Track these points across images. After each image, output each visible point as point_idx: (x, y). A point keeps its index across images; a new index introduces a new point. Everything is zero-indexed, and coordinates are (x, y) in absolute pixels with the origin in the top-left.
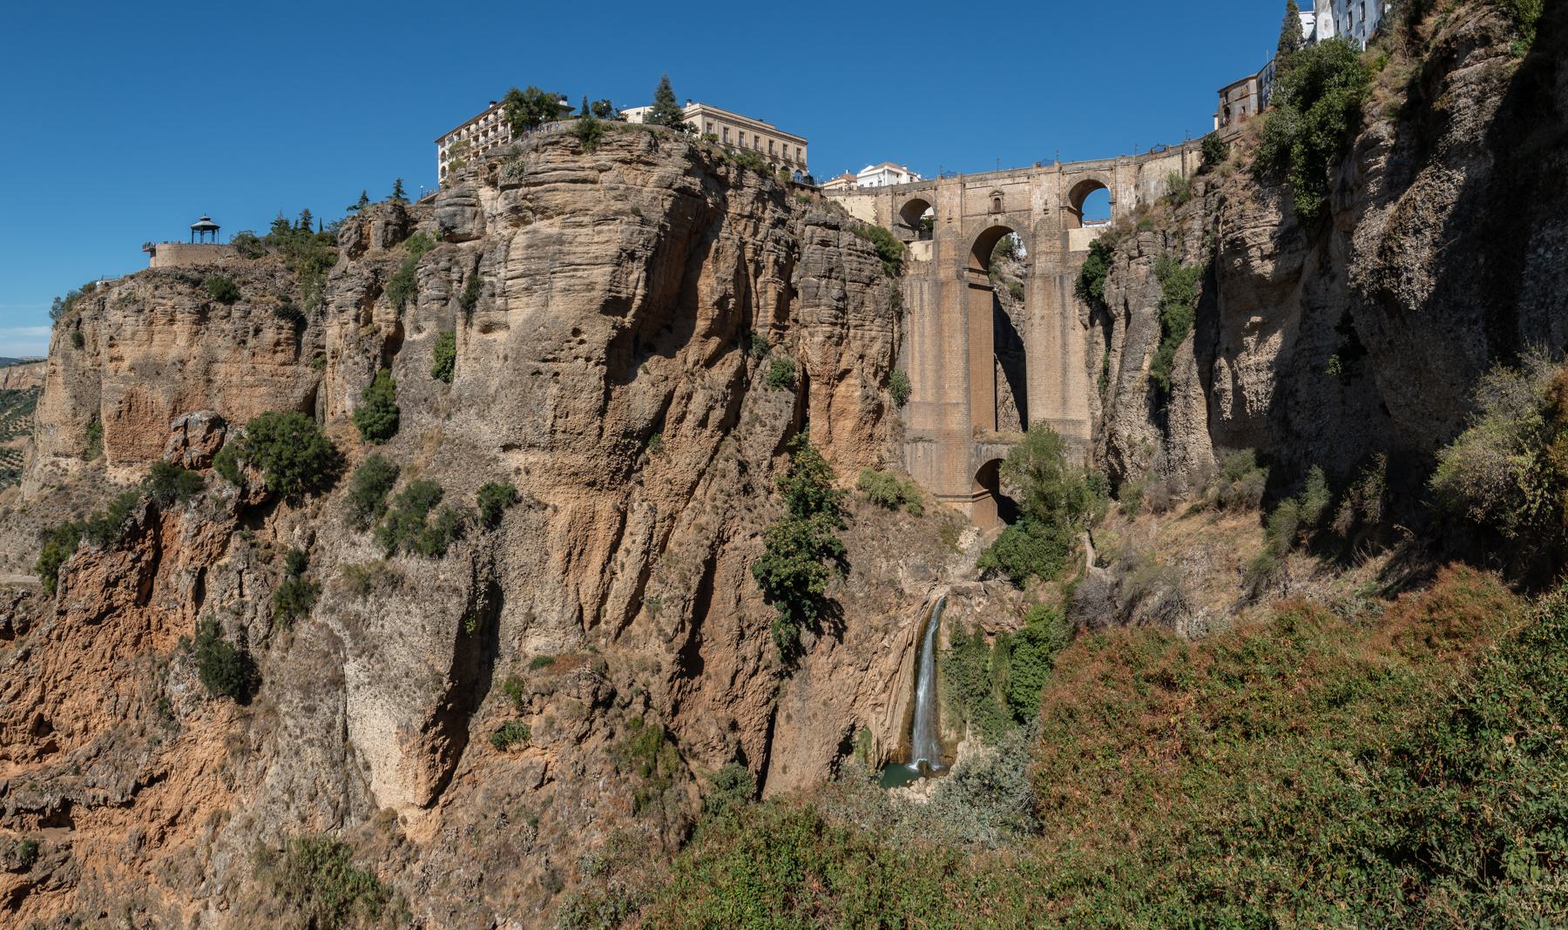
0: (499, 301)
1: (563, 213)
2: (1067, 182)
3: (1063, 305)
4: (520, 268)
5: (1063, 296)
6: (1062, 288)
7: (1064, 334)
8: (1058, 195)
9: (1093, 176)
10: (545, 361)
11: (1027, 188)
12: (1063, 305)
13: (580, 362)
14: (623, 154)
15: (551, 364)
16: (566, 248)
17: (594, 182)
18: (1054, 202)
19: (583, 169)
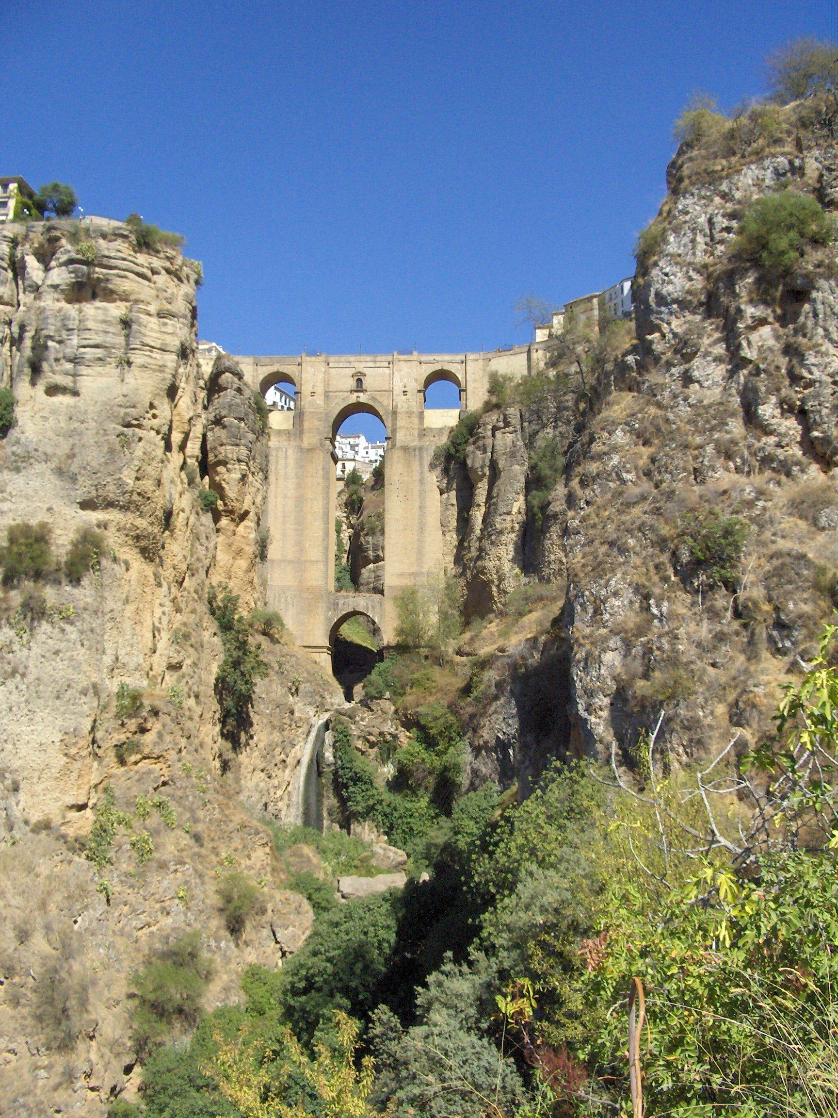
0: (69, 366)
1: (127, 300)
2: (427, 370)
3: (422, 473)
4: (97, 339)
5: (421, 465)
6: (421, 458)
7: (422, 493)
8: (416, 380)
9: (447, 367)
10: (128, 425)
11: (387, 371)
12: (422, 473)
13: (153, 433)
14: (168, 264)
15: (137, 430)
16: (142, 330)
17: (149, 280)
18: (414, 385)
19: (142, 266)
